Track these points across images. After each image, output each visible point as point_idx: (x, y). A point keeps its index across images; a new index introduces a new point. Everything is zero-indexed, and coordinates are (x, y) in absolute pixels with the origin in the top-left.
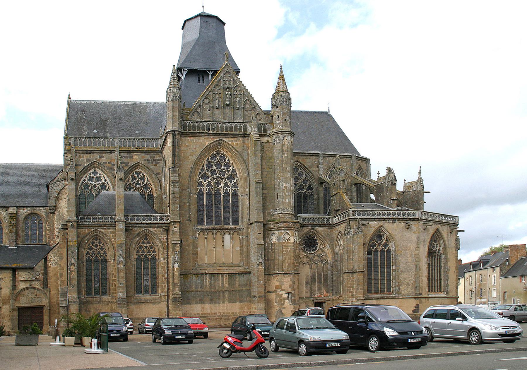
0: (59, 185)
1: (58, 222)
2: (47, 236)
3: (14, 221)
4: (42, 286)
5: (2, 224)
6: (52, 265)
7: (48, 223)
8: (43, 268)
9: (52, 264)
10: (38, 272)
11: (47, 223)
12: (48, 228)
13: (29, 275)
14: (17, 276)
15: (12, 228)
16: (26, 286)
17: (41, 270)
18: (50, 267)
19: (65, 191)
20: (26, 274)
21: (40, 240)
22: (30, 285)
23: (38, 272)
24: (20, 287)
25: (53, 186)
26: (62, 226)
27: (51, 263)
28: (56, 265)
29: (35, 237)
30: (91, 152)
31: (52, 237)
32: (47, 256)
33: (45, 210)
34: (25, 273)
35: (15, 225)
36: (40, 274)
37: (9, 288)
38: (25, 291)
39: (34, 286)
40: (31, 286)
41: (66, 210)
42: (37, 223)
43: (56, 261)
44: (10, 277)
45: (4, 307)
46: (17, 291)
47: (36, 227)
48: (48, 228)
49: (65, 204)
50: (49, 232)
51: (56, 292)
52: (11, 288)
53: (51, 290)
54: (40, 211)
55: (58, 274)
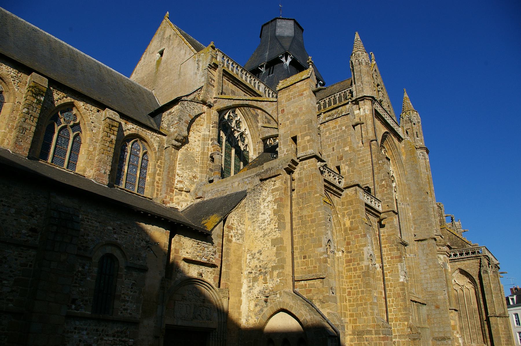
0: (193, 107)
1: (183, 166)
2: (155, 184)
3: (113, 134)
4: (217, 281)
5: (81, 132)
6: (234, 239)
7: (161, 163)
9: (235, 237)
11: (159, 162)
12: (158, 172)
15: (108, 147)
18: (230, 241)
19: (200, 120)
21: (141, 189)
25: (186, 105)
26: (291, 164)
27: (232, 233)
28: (240, 240)
29: (133, 180)
30: (238, 84)
31: (169, 190)
33: (158, 139)
35: (114, 142)
40: (200, 277)
41: (198, 149)
42: (141, 155)
43: (240, 232)
47: (138, 162)
48: (158, 172)
49: (199, 140)
51: (237, 299)
54: (152, 138)
55: (241, 261)
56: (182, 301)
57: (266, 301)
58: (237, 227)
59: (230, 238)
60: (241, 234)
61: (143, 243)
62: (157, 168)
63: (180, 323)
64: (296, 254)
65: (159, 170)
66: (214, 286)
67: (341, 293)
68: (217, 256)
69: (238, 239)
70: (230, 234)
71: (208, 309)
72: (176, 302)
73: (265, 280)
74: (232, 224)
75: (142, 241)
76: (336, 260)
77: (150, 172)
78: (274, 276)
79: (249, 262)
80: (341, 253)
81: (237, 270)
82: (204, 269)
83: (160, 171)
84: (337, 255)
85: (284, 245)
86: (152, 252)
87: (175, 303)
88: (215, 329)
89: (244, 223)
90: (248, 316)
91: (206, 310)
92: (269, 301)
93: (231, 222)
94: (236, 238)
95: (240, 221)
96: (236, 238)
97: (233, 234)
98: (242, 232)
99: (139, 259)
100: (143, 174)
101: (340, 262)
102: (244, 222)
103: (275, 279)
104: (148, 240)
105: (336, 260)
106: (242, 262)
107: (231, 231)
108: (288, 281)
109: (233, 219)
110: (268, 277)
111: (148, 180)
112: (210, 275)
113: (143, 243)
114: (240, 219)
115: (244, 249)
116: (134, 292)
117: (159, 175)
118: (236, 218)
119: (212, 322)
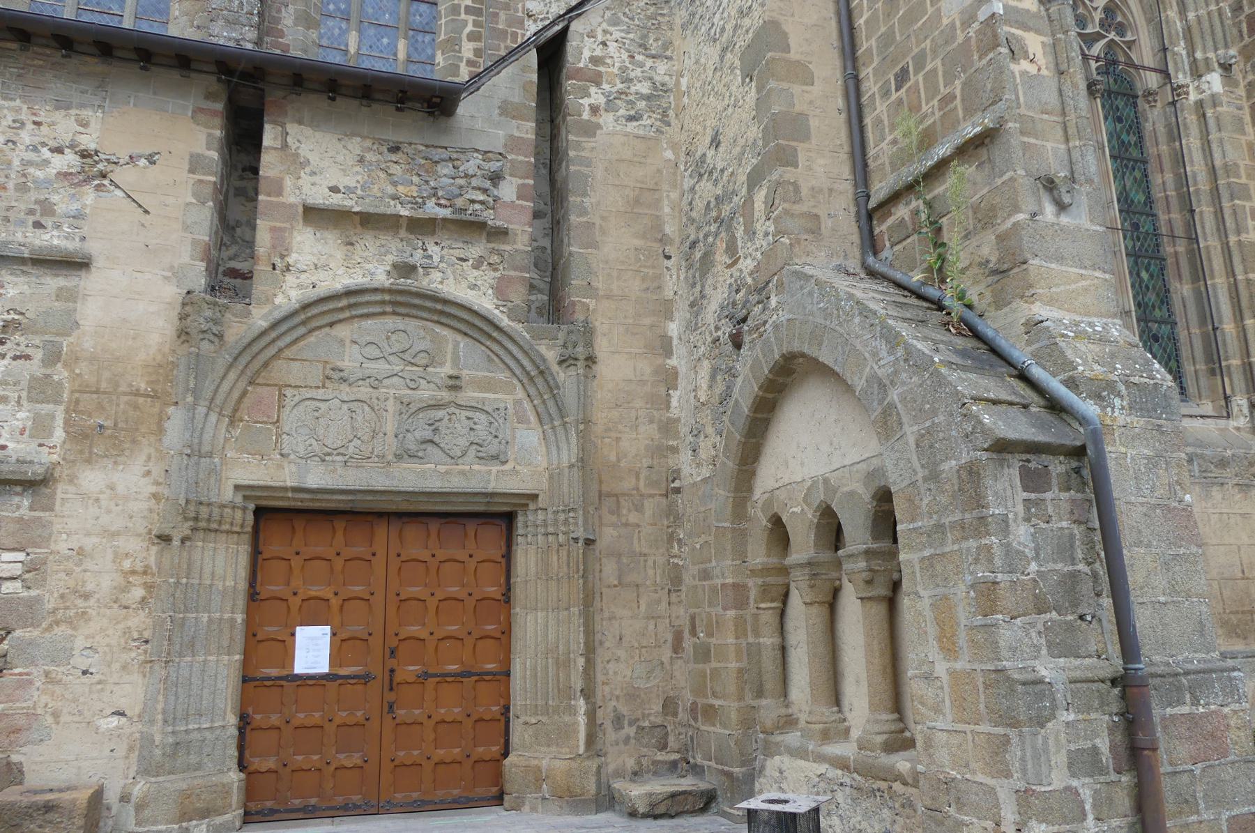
4: (518, 296)
6: (607, 120)
8: (527, 130)
9: (610, 105)
10: (477, 159)
12: (470, 28)
13: (396, 170)
14: (269, 164)
16: (356, 279)
17: (514, 143)
18: (590, 130)
20: (361, 160)
22: (406, 270)
23: (477, 159)
24: (290, 279)
32: (565, 30)
34: (356, 145)
36: (496, 178)
37: (176, 274)
38: (342, 331)
39: (434, 282)
43: (644, 88)
44: (196, 164)
45: (92, 479)
46: (260, 318)
48: (470, 28)
50: (478, 52)
51: (646, 367)
52: (198, 278)
53: (602, 347)
55: (657, 204)
56: (324, 387)
57: (738, 345)
58: (623, 69)
59: (586, 116)
60: (648, 98)
61: (69, 160)
62: (463, 16)
63: (316, 478)
64: (871, 86)
65: (474, 20)
66: (505, 322)
67: (1239, 269)
68: (508, 190)
69: (631, 119)
70: (585, 102)
71: (478, 416)
72: (289, 392)
73: (731, 249)
74: (595, 60)
75: (59, 150)
76: (1191, 119)
77: (443, 37)
78: (756, 215)
79: (690, 204)
80: (1214, 81)
81: (638, 243)
82: (437, 249)
83: (475, 24)
84: (1193, 97)
85: (794, 55)
86: (119, 193)
87: (282, 396)
88: (534, 497)
89: (668, 53)
90: (697, 432)
91: (468, 418)
92: (747, 339)
93: (586, 54)
94: (622, 112)
95: (643, 46)
96: (622, 112)
97: (601, 100)
98: (655, 89)
99: (38, 225)
100: (423, 50)
101: (1212, 123)
102: (666, 46)
103: (758, 226)
104: (92, 146)
105: (1191, 119)
106: (667, 210)
107: (593, 90)
108: (827, 224)
109: (600, 38)
110: (740, 233)
111: (439, 64)
112: (476, 273)
113: (69, 160)
114: (645, 37)
115: (669, 154)
116: (15, 358)
117: (472, 37)
118: (617, 35)
119: (508, 467)
